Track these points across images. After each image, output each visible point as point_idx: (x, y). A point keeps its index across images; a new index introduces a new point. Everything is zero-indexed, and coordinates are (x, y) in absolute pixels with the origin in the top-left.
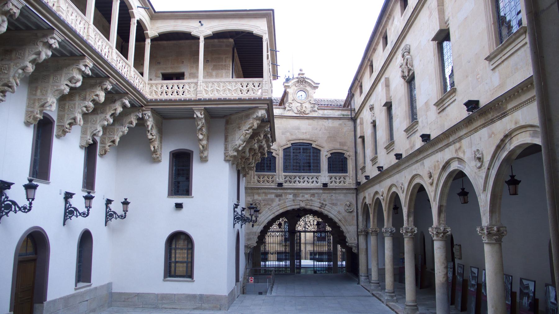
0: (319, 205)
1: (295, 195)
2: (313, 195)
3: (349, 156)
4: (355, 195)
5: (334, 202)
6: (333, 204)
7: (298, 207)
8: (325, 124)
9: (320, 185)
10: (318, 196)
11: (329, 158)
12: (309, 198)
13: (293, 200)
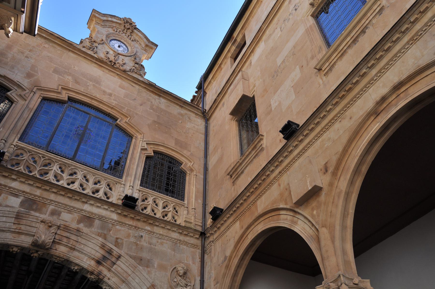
0: (99, 253)
1: (30, 203)
2: (88, 219)
3: (192, 170)
4: (198, 252)
5: (145, 255)
6: (140, 260)
7: (25, 241)
8: (153, 101)
9: (116, 197)
10: (102, 227)
11: (148, 158)
12: (74, 225)
13: (18, 216)
